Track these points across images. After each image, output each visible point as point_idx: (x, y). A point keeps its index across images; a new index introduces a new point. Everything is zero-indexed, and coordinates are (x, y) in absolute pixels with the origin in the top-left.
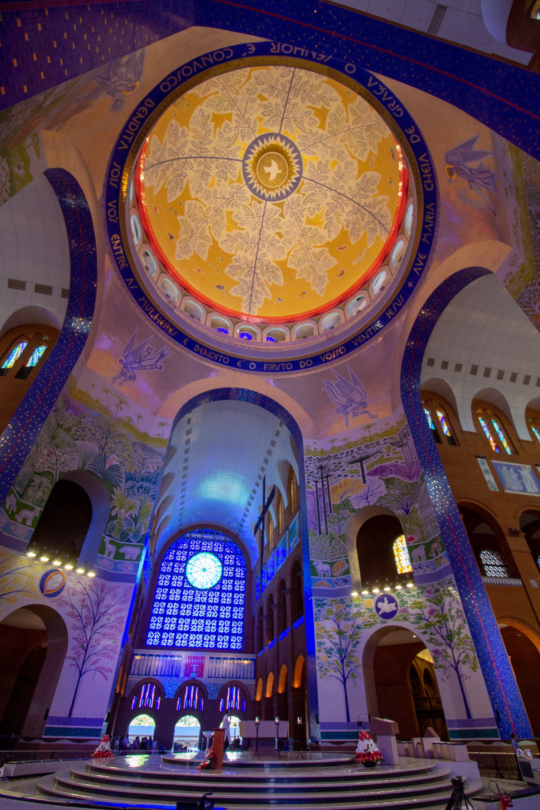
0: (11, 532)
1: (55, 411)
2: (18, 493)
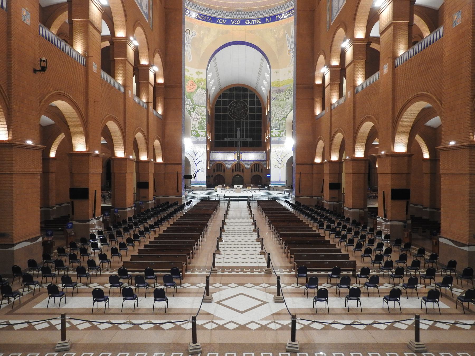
0: (281, 140)
1: (274, 99)
2: (277, 130)
